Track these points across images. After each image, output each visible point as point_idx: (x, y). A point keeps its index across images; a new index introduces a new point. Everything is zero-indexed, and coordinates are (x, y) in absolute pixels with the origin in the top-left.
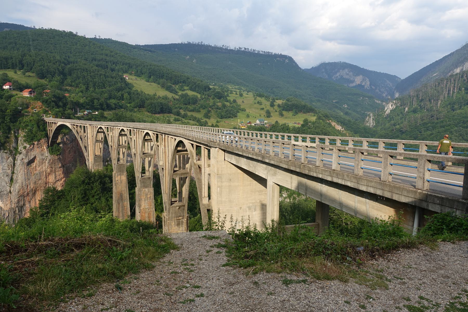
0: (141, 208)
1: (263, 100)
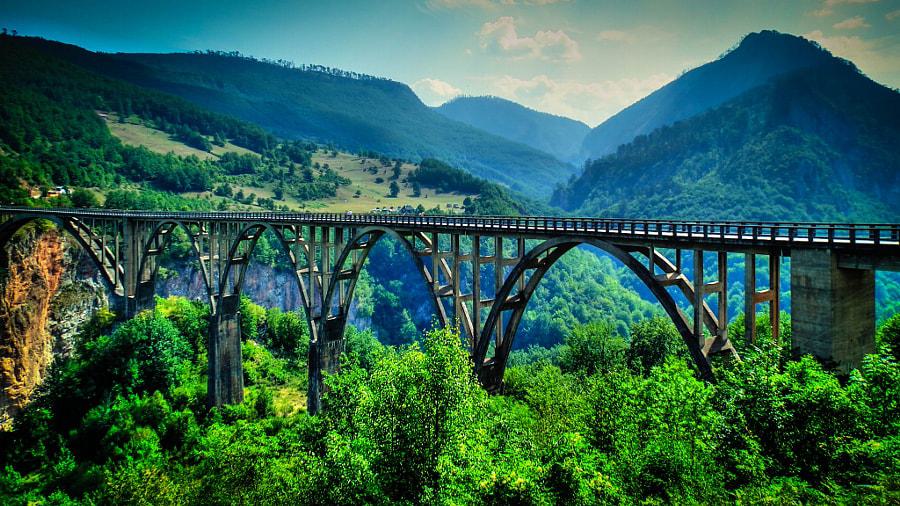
1: (375, 162)
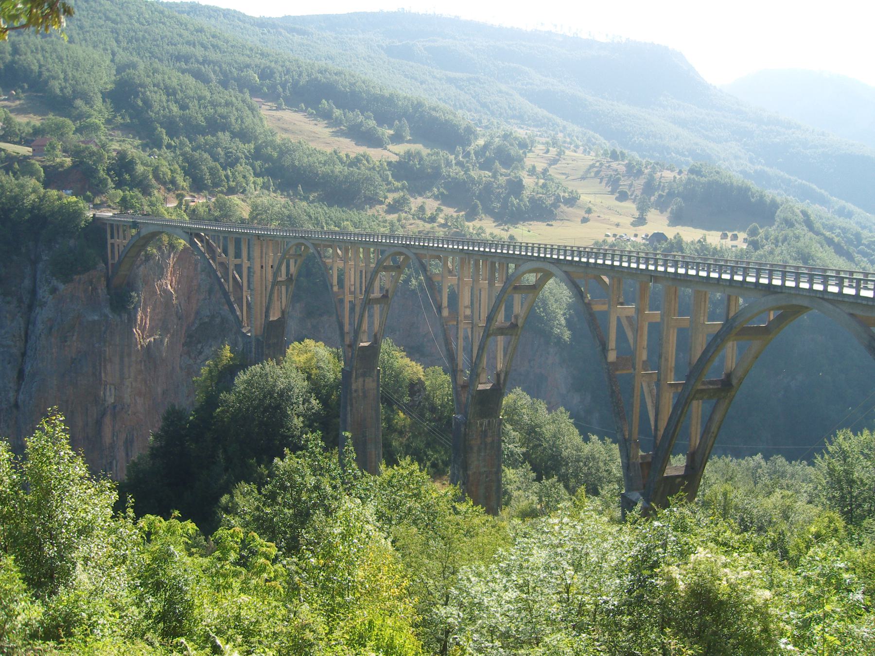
0: (470, 473)
